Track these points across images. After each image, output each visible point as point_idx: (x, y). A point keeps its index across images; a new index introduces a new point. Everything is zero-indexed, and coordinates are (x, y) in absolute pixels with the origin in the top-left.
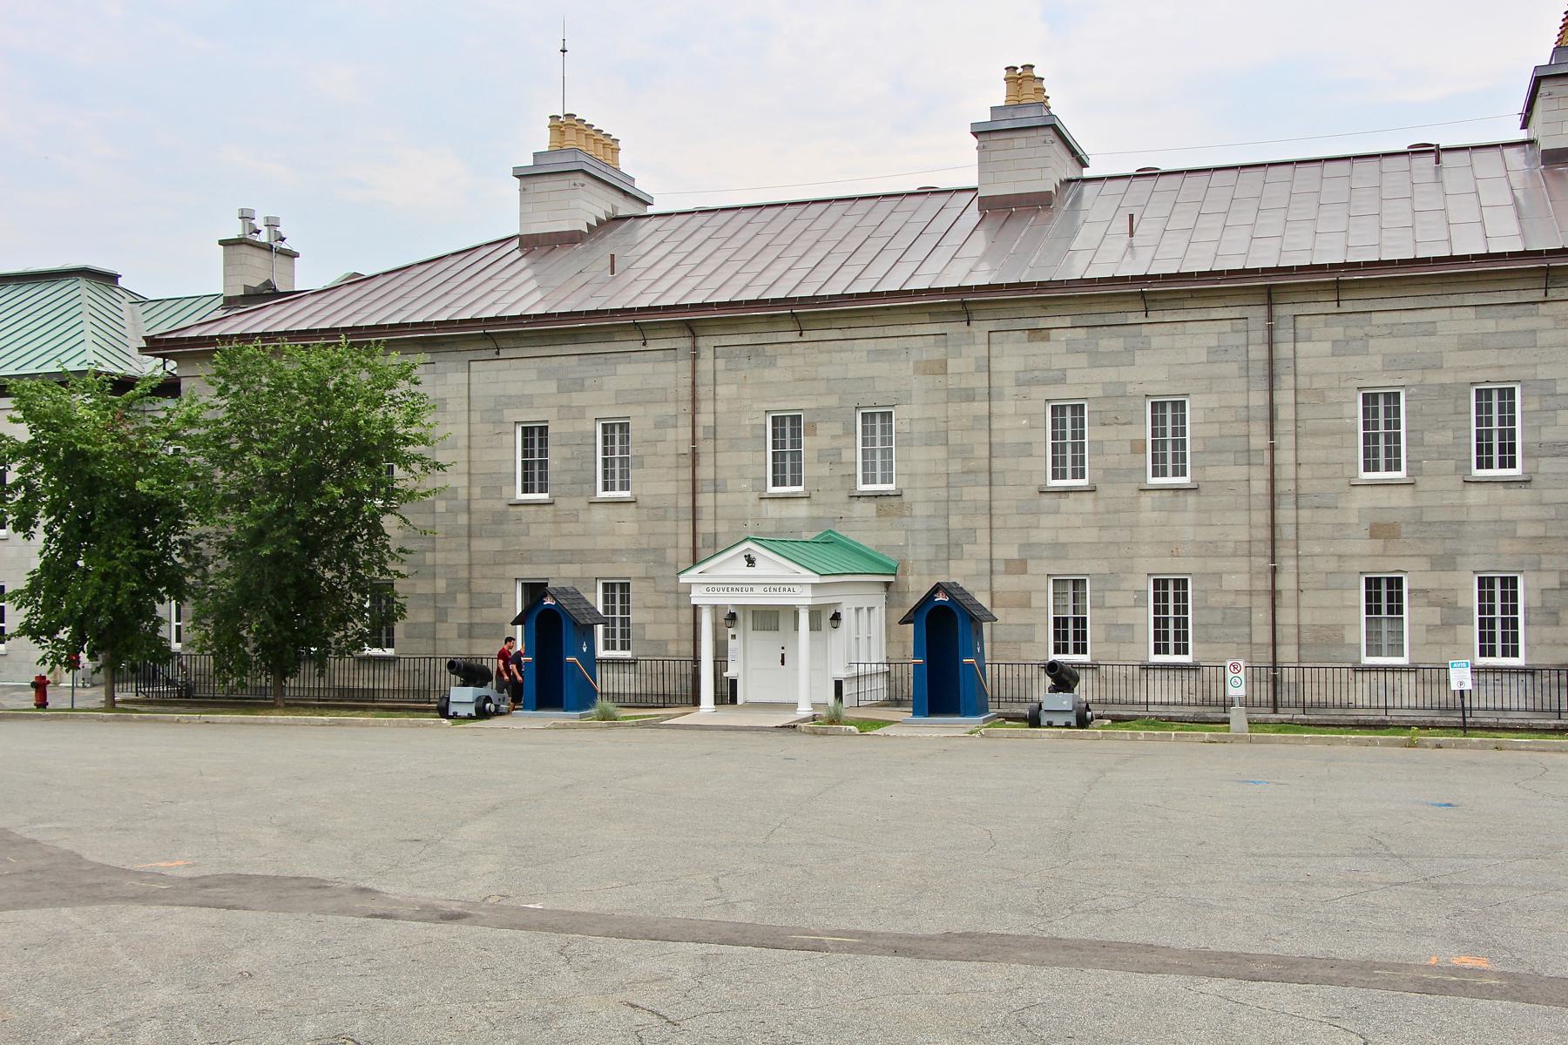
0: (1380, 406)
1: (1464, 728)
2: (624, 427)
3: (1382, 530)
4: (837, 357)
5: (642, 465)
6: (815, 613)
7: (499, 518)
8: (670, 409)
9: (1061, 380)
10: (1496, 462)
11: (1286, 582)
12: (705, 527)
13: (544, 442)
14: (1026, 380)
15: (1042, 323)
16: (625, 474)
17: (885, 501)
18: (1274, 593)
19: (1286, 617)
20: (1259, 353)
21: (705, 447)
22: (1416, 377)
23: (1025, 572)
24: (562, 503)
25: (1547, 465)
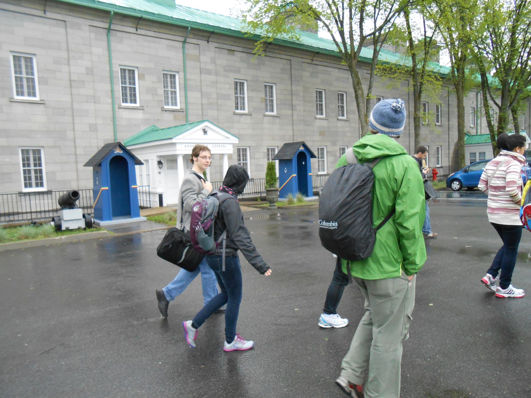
15: (233, 48)
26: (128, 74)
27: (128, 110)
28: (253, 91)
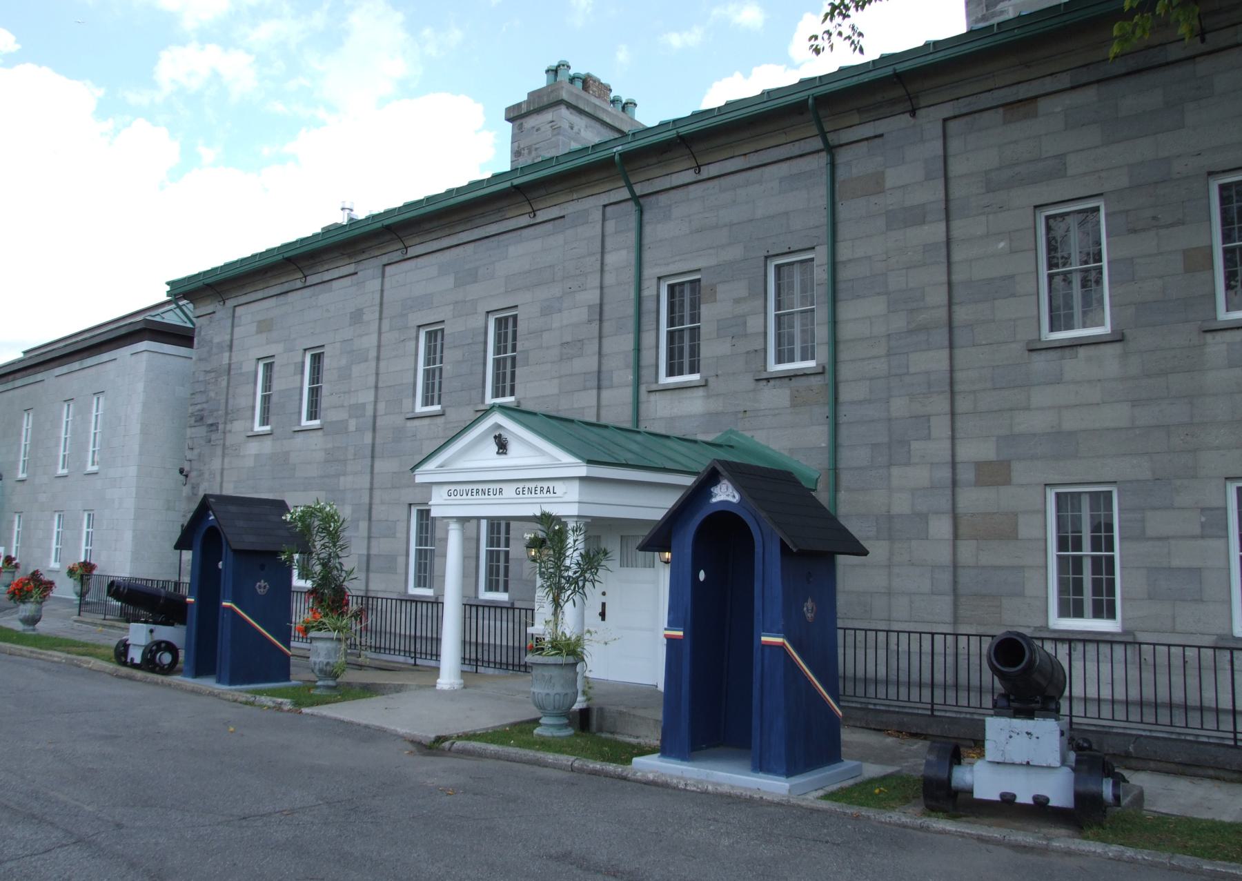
15: (1024, 91)
17: (803, 382)
23: (1007, 482)
26: (686, 297)
27: (668, 393)
28: (1134, 231)
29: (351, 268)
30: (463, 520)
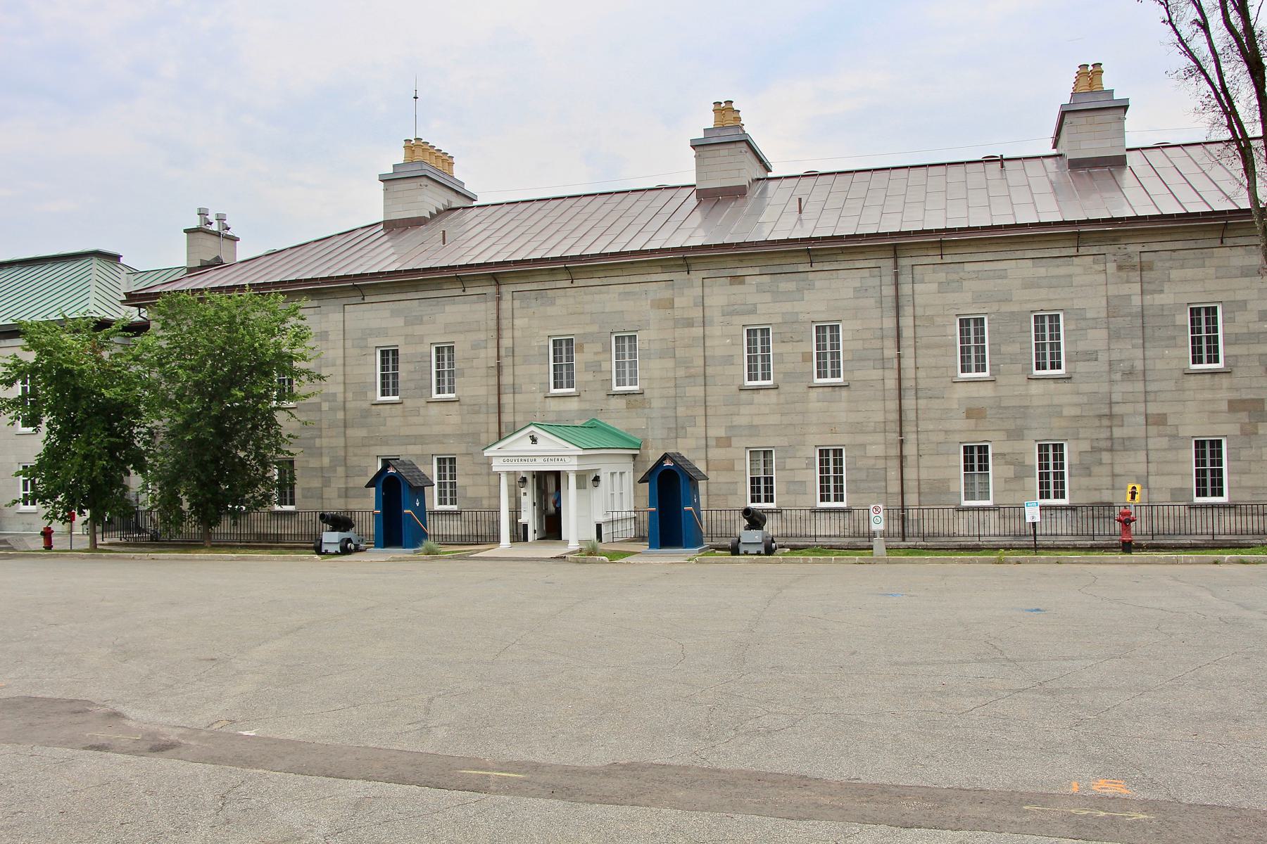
0: (971, 327)
1: (1036, 548)
2: (451, 349)
3: (974, 413)
4: (597, 297)
5: (463, 375)
6: (581, 476)
7: (365, 414)
8: (482, 336)
9: (753, 311)
10: (1048, 365)
11: (910, 450)
12: (507, 418)
13: (396, 361)
14: (730, 312)
15: (739, 272)
16: (451, 382)
18: (902, 458)
19: (910, 474)
20: (889, 291)
21: (506, 362)
22: (995, 307)
23: (730, 446)
24: (408, 403)
25: (1082, 367)
29: (315, 303)
30: (508, 473)
